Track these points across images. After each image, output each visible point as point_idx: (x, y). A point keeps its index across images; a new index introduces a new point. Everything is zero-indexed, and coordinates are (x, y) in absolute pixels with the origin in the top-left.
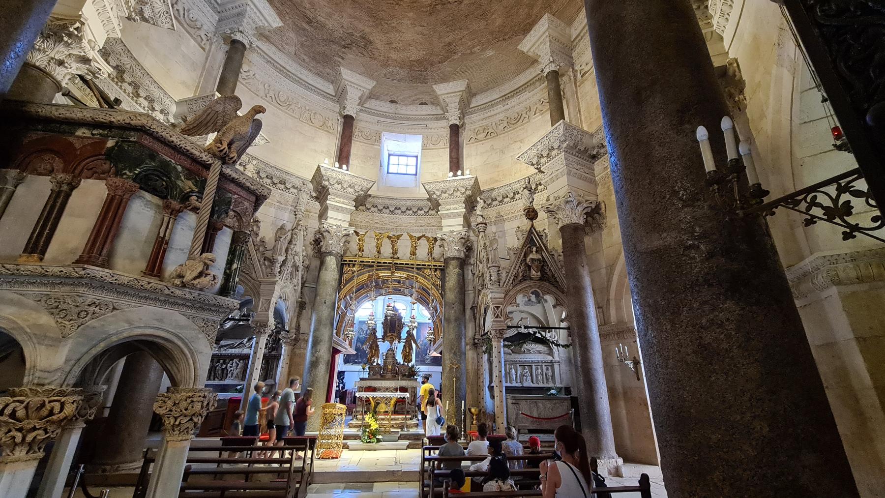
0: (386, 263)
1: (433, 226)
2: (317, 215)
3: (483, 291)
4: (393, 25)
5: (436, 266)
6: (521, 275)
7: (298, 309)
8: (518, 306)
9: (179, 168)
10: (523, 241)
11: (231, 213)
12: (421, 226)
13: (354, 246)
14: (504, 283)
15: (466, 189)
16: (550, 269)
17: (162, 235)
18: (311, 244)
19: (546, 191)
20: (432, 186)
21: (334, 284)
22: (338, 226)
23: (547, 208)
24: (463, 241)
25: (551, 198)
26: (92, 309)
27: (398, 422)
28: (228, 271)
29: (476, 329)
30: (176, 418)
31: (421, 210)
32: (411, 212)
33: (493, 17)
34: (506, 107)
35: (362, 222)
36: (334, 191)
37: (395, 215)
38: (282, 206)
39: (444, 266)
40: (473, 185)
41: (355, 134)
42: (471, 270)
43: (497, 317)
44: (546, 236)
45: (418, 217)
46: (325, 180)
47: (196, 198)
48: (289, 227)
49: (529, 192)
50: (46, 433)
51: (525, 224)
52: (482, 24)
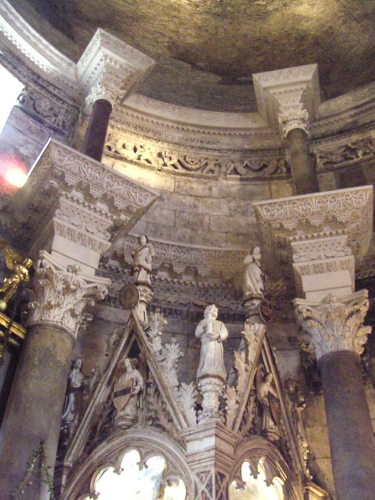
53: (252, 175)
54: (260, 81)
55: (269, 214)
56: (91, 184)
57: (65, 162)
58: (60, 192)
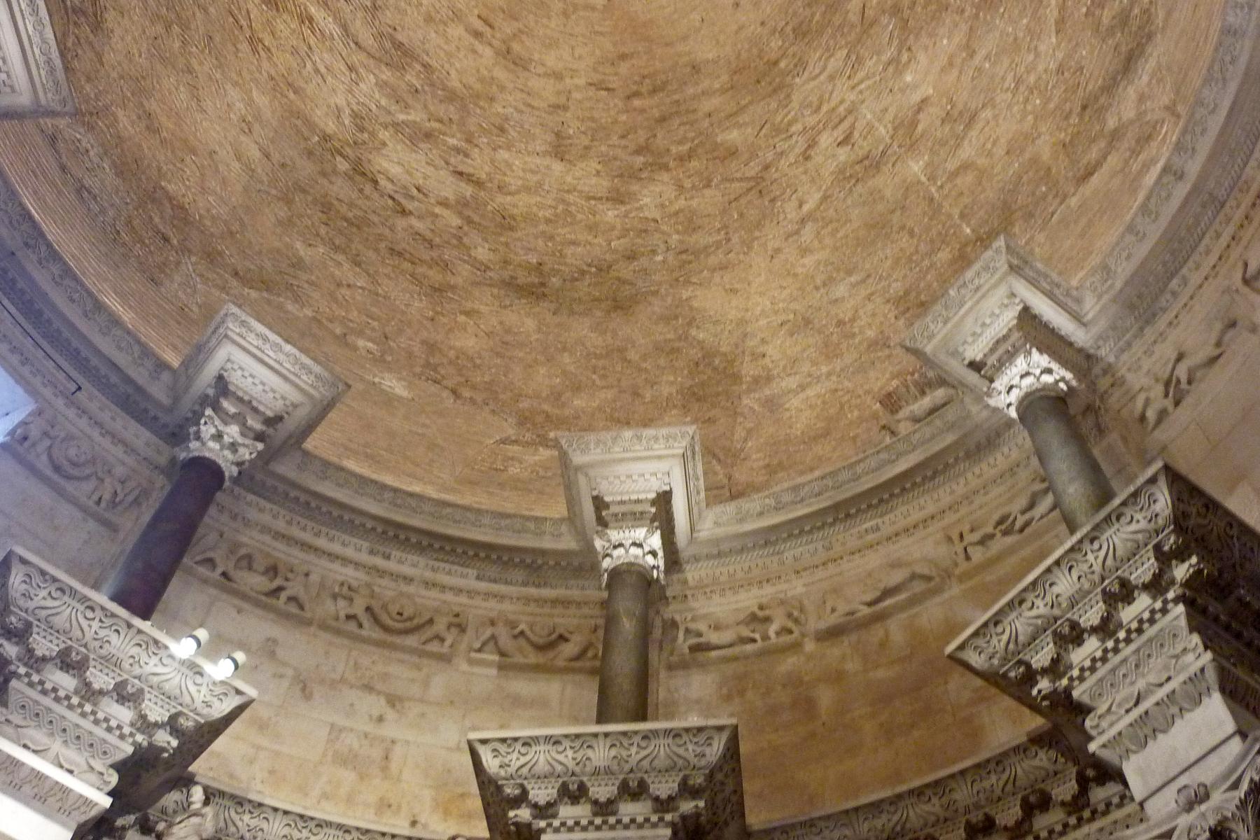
4: (194, 63)
33: (462, 318)
34: (379, 561)
52: (419, 306)
53: (533, 658)
54: (570, 452)
55: (497, 762)
56: (92, 656)
57: (38, 602)
58: (13, 668)
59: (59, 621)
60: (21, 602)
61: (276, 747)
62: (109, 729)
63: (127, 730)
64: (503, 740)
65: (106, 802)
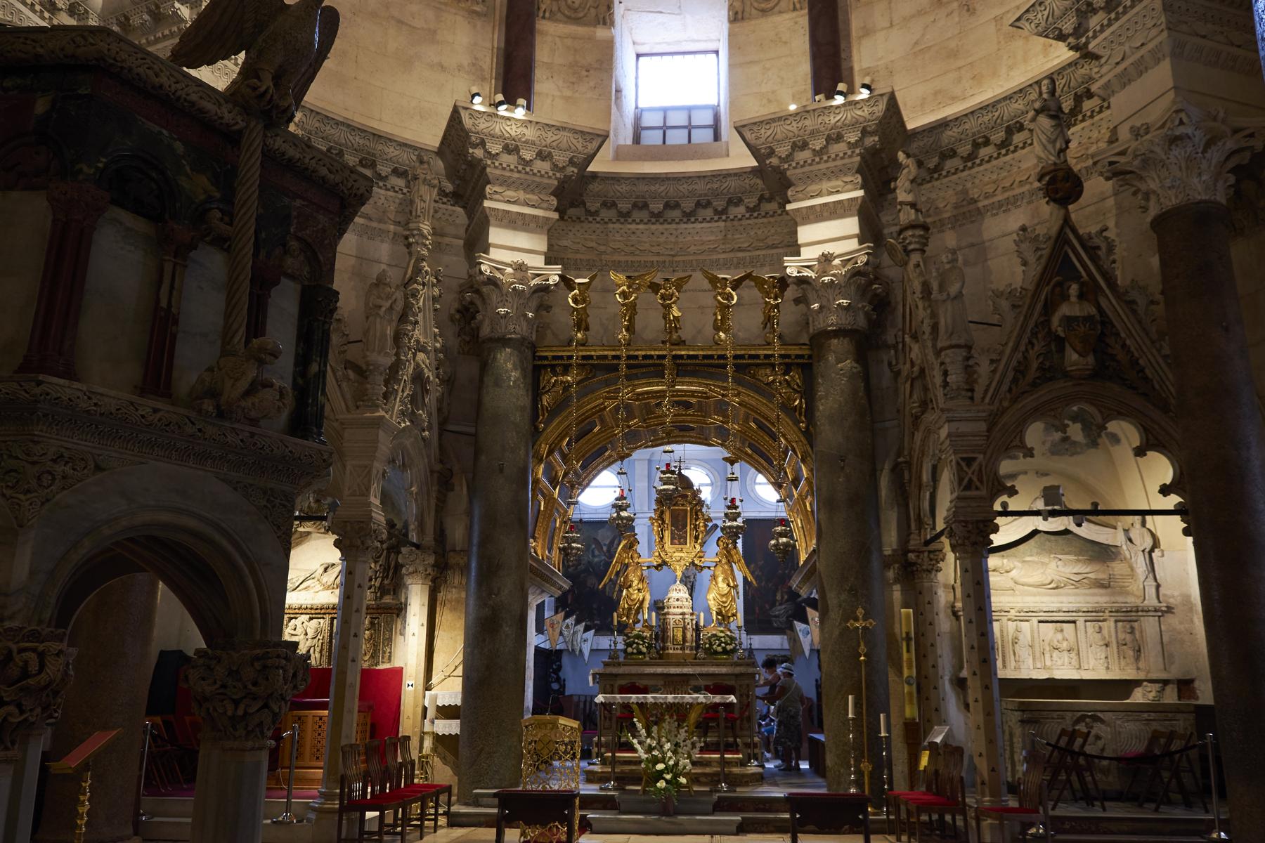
0: (651, 357)
1: (773, 246)
2: (461, 242)
3: (930, 417)
5: (788, 356)
6: (1035, 365)
7: (435, 488)
8: (1029, 453)
9: (179, 147)
10: (1039, 269)
11: (294, 244)
12: (740, 250)
13: (562, 319)
14: (986, 391)
15: (865, 132)
16: (1124, 345)
17: (164, 303)
18: (452, 319)
19: (1106, 113)
20: (765, 133)
21: (520, 418)
22: (520, 267)
23: (1111, 163)
24: (863, 280)
25: (1124, 134)
26: (59, 469)
27: (708, 770)
28: (300, 381)
29: (909, 526)
30: (236, 703)
31: (737, 205)
32: (709, 212)
35: (577, 251)
36: (498, 172)
37: (666, 226)
38: (374, 224)
39: (810, 357)
40: (884, 117)
41: (543, 7)
42: (890, 364)
43: (968, 488)
44: (1111, 249)
45: (729, 224)
46: (475, 146)
47: (219, 215)
48: (394, 276)
49: (1053, 123)
50: (22, 712)
51: (1045, 214)
58: (782, 168)
59: (779, 136)
60: (759, 142)
61: (970, 60)
62: (842, 158)
63: (849, 152)
64: (1027, 11)
65: (860, 193)
